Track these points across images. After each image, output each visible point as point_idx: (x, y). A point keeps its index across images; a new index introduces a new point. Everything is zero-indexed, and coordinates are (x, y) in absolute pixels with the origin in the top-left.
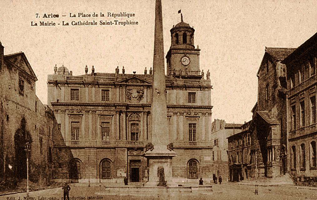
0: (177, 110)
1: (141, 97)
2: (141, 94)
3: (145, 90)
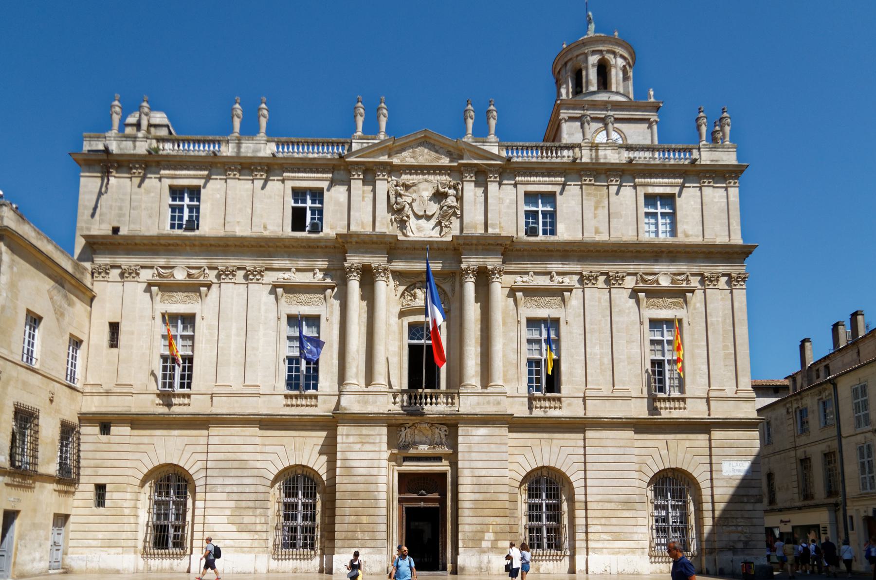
2: (451, 201)
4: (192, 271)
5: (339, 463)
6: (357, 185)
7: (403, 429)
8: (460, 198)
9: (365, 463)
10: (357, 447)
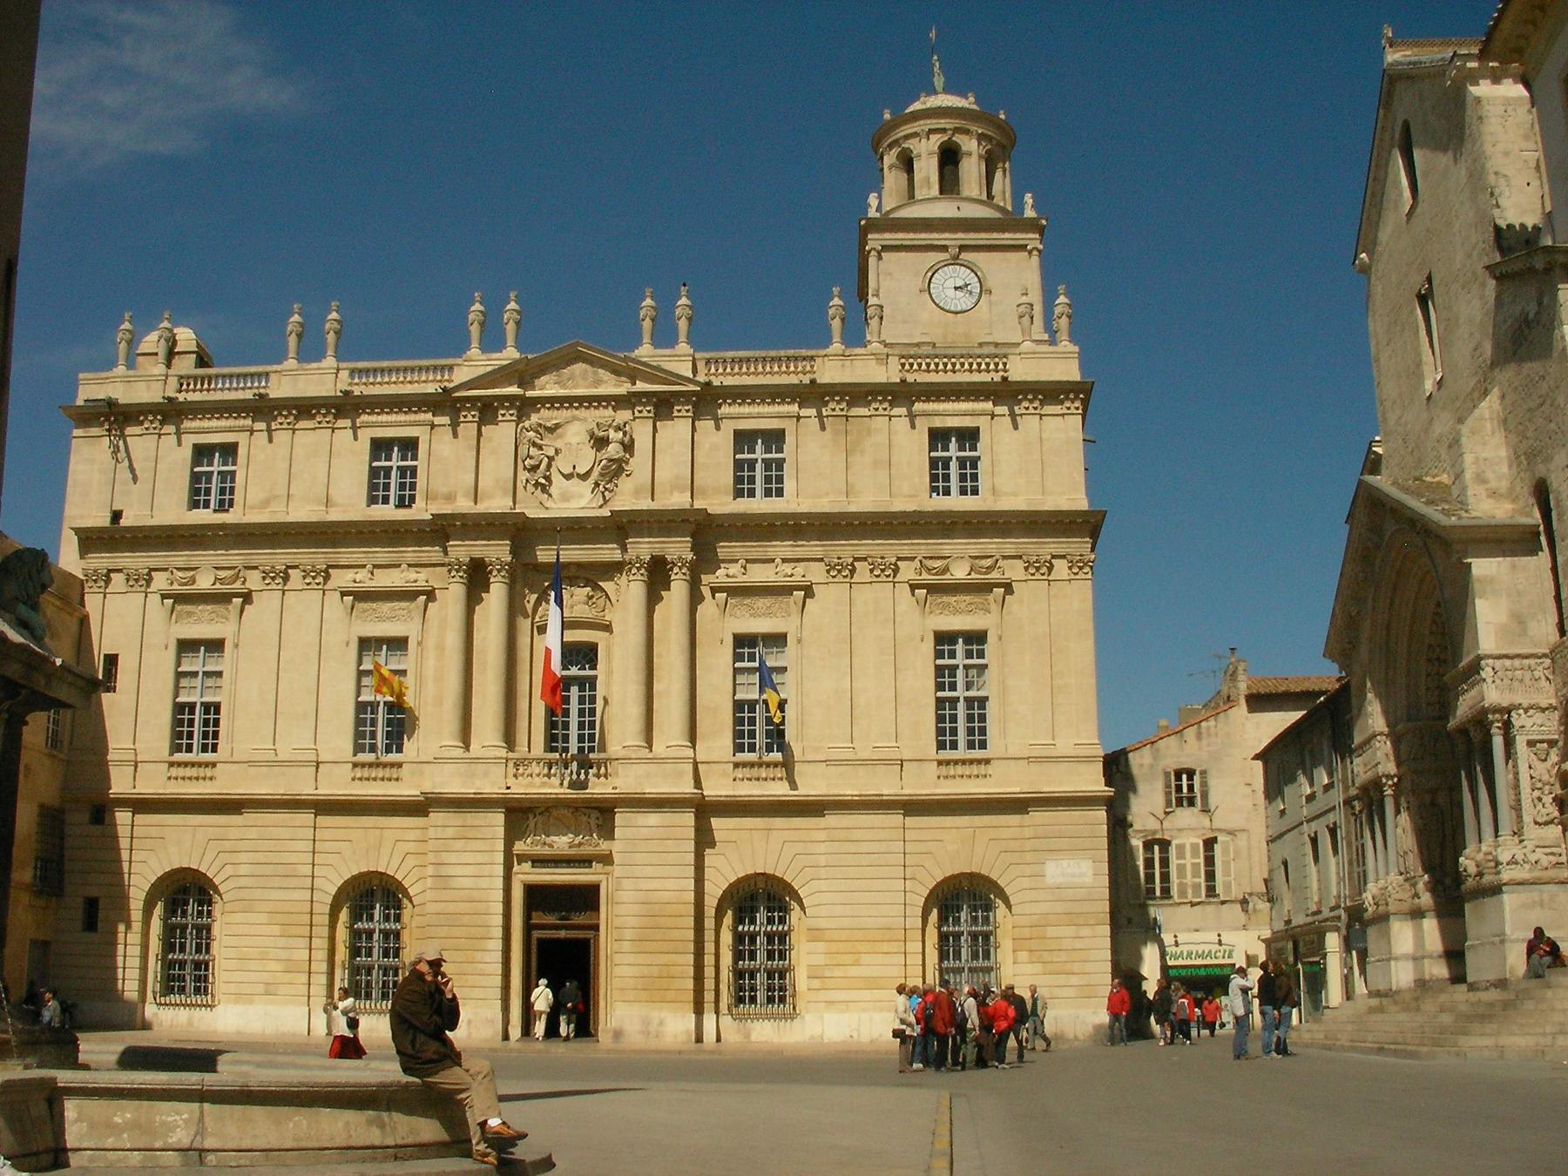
0: (845, 549)
1: (616, 470)
2: (613, 450)
3: (642, 433)
4: (222, 574)
6: (468, 429)
8: (629, 447)
9: (469, 870)
10: (459, 844)
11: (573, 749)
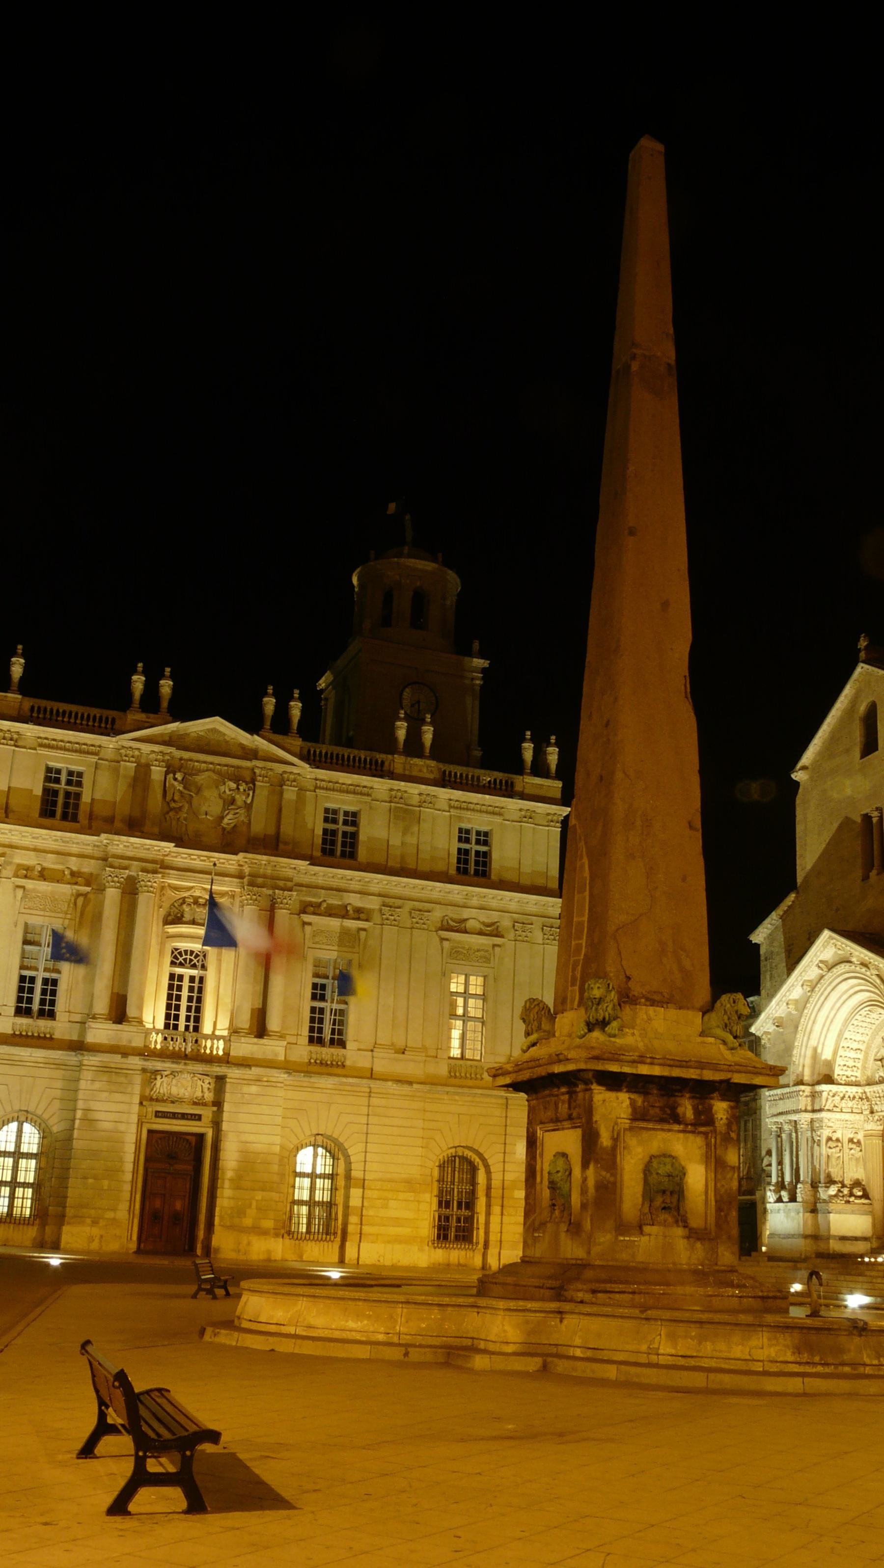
5: (79, 1114)
7: (159, 1077)
11: (182, 1028)
